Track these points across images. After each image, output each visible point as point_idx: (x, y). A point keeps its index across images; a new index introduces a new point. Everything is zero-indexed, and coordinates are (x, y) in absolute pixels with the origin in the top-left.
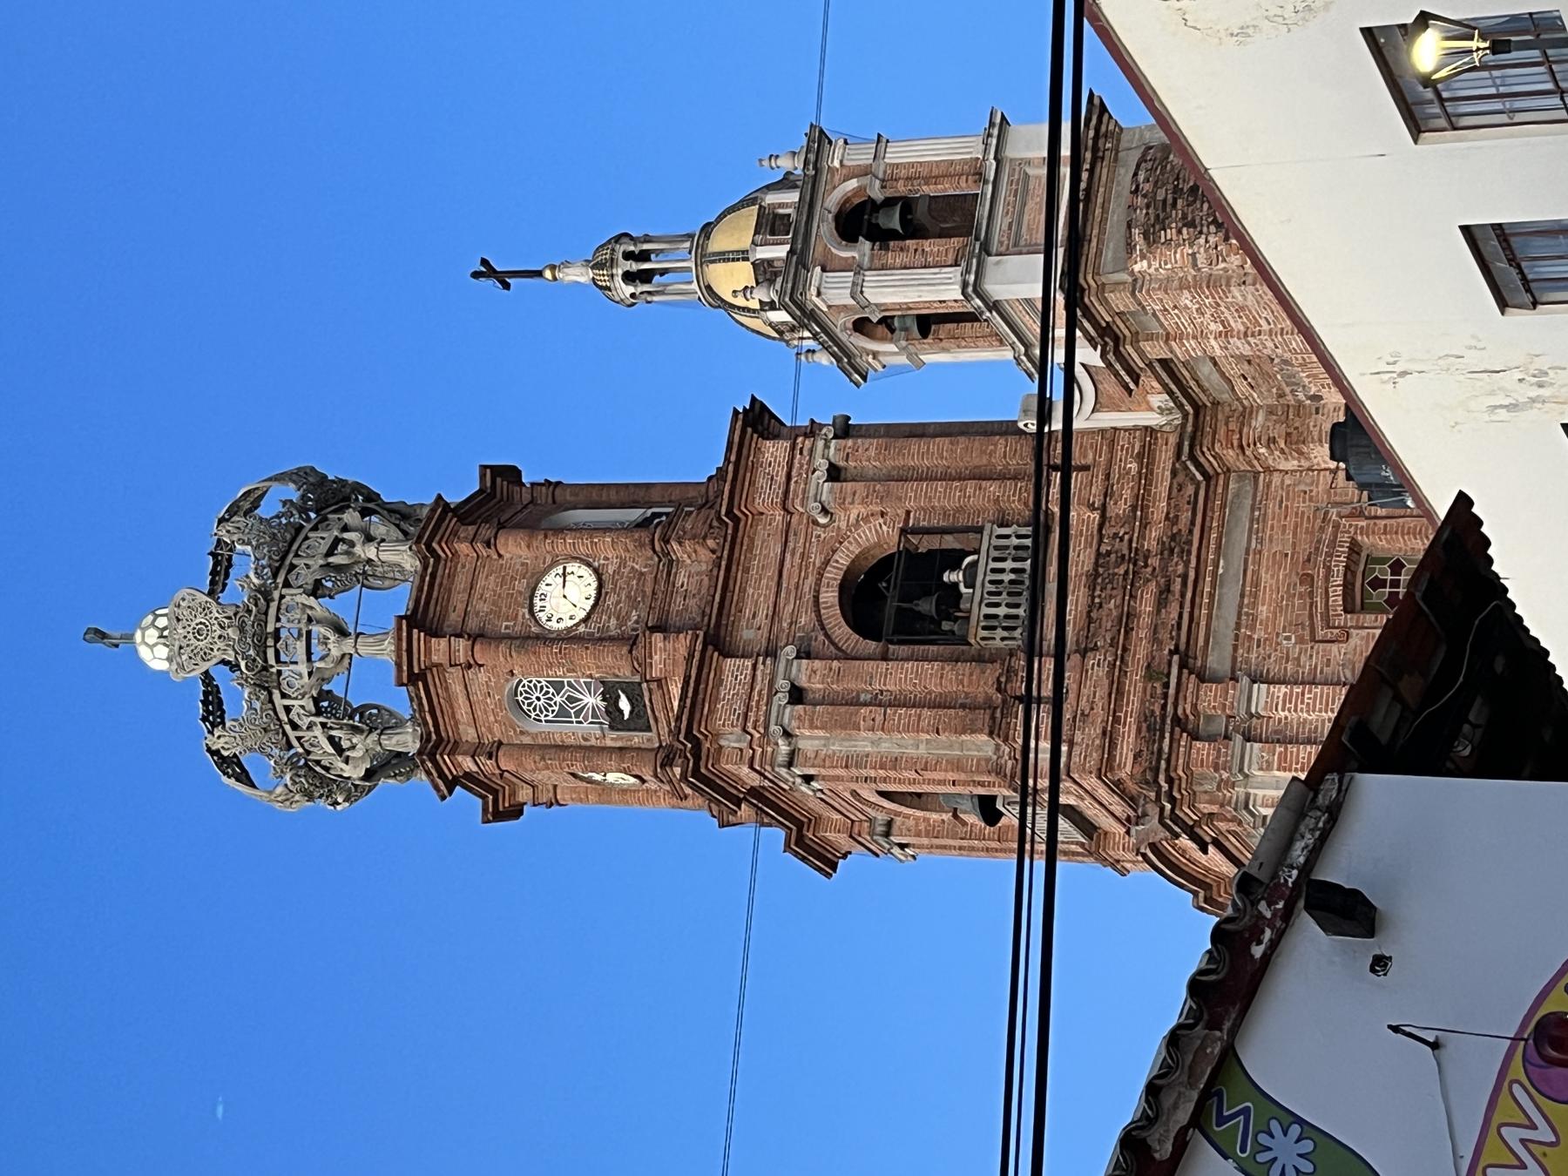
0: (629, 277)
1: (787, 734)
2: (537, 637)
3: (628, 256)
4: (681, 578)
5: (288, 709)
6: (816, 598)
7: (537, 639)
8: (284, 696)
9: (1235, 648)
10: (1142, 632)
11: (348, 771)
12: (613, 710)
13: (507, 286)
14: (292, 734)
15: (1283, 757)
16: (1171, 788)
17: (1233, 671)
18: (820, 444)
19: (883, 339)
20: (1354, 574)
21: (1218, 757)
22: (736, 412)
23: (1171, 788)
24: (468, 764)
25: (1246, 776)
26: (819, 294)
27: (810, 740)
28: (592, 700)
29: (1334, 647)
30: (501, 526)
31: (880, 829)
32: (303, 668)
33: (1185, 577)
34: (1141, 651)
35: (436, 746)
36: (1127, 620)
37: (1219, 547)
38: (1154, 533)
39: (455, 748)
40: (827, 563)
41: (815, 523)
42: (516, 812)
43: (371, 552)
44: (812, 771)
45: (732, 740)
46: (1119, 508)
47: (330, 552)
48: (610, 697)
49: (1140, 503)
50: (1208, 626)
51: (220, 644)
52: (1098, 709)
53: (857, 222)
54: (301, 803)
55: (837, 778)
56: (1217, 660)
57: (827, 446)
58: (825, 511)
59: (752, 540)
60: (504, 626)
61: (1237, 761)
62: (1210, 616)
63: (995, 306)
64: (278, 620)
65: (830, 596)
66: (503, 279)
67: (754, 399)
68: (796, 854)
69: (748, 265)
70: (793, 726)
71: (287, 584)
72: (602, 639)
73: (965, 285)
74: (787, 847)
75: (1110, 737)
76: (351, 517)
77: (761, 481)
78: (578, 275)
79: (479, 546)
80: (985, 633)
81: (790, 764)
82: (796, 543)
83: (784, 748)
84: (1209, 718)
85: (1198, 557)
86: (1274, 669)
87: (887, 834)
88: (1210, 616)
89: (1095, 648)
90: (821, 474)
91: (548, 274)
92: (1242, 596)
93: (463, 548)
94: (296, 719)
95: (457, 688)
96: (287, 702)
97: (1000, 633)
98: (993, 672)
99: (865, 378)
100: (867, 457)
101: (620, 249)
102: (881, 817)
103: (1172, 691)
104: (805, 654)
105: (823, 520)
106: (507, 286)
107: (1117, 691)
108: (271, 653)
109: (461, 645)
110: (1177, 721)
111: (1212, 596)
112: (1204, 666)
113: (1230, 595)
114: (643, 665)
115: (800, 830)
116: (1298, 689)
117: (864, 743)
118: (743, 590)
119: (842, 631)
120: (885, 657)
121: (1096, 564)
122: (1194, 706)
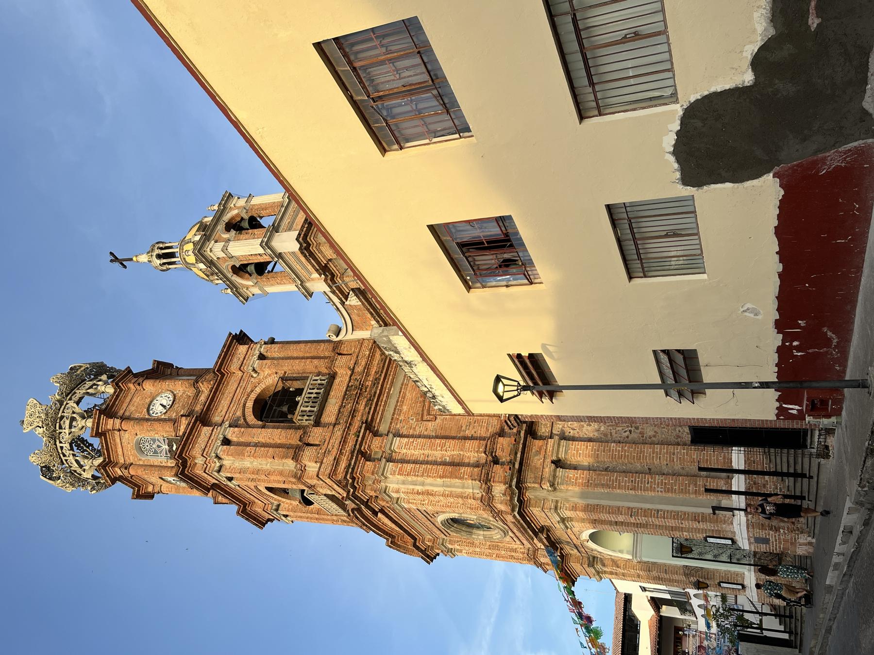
0: (159, 257)
1: (217, 457)
2: (147, 420)
3: (161, 249)
5: (62, 448)
9: (391, 423)
13: (125, 267)
14: (63, 458)
15: (401, 469)
16: (353, 482)
17: (389, 432)
18: (259, 346)
19: (247, 279)
22: (230, 334)
23: (353, 482)
25: (386, 478)
26: (211, 251)
27: (227, 462)
28: (166, 447)
29: (430, 423)
30: (147, 378)
31: (274, 507)
32: (67, 431)
33: (375, 393)
34: (356, 423)
35: (107, 464)
36: (353, 413)
37: (392, 382)
38: (371, 378)
39: (116, 464)
40: (252, 391)
42: (150, 496)
44: (229, 475)
45: (200, 461)
46: (359, 369)
47: (91, 387)
49: (367, 367)
50: (382, 414)
51: (38, 420)
52: (335, 450)
54: (70, 489)
55: (241, 479)
56: (383, 429)
58: (256, 372)
59: (228, 383)
60: (137, 415)
61: (381, 470)
62: (383, 410)
63: (280, 256)
65: (250, 404)
67: (241, 331)
69: (191, 244)
70: (221, 454)
71: (70, 399)
73: (262, 241)
75: (337, 461)
76: (104, 377)
77: (235, 360)
78: (143, 258)
81: (219, 471)
82: (243, 384)
83: (218, 464)
84: (376, 453)
85: (382, 386)
87: (277, 510)
89: (339, 424)
90: (256, 357)
91: (134, 259)
92: (397, 402)
93: (131, 385)
94: (64, 451)
95: (118, 440)
97: (306, 417)
98: (300, 432)
99: (246, 300)
100: (274, 351)
101: (157, 246)
102: (276, 503)
103: (360, 439)
105: (255, 375)
106: (125, 267)
107: (344, 441)
108: (58, 425)
109: (118, 421)
110: (360, 451)
111: (386, 402)
112: (378, 430)
113: (392, 402)
114: (176, 430)
115: (245, 507)
116: (411, 440)
118: (220, 401)
119: (251, 418)
120: (263, 427)
122: (369, 446)
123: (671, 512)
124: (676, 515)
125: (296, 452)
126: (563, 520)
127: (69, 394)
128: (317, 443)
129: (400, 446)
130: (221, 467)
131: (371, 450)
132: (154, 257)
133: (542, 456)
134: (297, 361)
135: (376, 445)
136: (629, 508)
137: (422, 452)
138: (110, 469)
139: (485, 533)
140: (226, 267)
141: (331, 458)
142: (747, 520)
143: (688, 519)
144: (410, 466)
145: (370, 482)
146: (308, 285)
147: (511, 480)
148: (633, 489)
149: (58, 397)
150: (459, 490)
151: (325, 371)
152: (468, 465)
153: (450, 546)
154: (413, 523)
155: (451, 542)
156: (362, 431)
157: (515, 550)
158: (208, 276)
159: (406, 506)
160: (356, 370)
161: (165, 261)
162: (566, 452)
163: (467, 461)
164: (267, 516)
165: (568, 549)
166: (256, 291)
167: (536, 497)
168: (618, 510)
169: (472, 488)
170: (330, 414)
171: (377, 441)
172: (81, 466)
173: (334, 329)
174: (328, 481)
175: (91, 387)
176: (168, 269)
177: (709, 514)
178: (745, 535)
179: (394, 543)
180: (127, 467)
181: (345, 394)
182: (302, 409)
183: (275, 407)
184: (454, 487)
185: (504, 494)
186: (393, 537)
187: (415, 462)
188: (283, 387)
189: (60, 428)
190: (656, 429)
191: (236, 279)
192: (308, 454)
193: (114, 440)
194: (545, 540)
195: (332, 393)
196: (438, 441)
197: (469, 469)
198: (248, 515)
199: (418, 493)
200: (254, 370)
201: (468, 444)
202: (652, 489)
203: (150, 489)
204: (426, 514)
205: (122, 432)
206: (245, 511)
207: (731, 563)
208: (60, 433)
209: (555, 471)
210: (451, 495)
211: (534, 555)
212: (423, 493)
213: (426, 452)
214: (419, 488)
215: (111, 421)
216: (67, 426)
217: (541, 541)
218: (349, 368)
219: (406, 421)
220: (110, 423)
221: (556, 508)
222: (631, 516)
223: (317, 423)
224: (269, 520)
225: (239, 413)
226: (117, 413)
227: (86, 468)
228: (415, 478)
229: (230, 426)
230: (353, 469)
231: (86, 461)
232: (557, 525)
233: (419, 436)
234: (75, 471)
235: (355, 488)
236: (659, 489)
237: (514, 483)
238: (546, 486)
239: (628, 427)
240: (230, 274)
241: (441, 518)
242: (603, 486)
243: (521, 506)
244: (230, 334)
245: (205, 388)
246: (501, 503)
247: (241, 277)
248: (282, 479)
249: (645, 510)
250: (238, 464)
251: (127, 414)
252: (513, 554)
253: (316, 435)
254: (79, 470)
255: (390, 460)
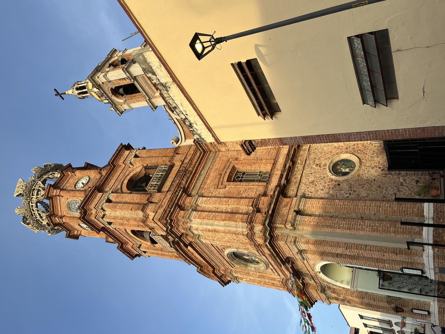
0: (77, 89)
5: (32, 206)
6: (123, 182)
8: (32, 203)
9: (199, 190)
13: (63, 99)
14: (33, 212)
15: (200, 215)
20: (233, 175)
21: (184, 215)
22: (121, 144)
25: (191, 221)
26: (98, 78)
29: (222, 190)
32: (35, 197)
39: (57, 216)
40: (128, 175)
41: (130, 167)
45: (94, 211)
46: (186, 161)
47: (51, 174)
49: (191, 160)
51: (21, 190)
54: (36, 231)
56: (194, 193)
57: (136, 151)
58: (132, 165)
59: (117, 171)
60: (69, 188)
61: (188, 215)
62: (196, 183)
64: (35, 187)
65: (126, 182)
67: (129, 144)
68: (121, 251)
70: (104, 207)
71: (40, 180)
74: (118, 248)
80: (149, 188)
82: (124, 171)
83: (103, 214)
84: (188, 206)
87: (139, 248)
88: (196, 183)
90: (133, 156)
91: (66, 92)
92: (204, 178)
93: (69, 173)
96: (32, 204)
98: (148, 196)
100: (143, 154)
102: (139, 243)
103: (178, 197)
105: (131, 167)
109: (58, 191)
110: (177, 204)
112: (191, 194)
113: (202, 178)
116: (209, 199)
119: (125, 189)
121: (177, 173)
123: (376, 247)
124: (380, 249)
126: (301, 252)
127: (40, 177)
128: (157, 202)
129: (202, 203)
130: (104, 215)
131: (185, 205)
132: (75, 89)
133: (288, 208)
135: (188, 201)
136: (345, 243)
137: (214, 206)
138: (53, 218)
139: (256, 266)
140: (107, 89)
141: (162, 210)
142: (434, 253)
143: (388, 252)
145: (182, 223)
146: (153, 100)
147: (265, 220)
148: (349, 229)
149: (33, 179)
150: (234, 229)
152: (242, 213)
153: (236, 275)
154: (212, 257)
155: (236, 272)
156: (181, 192)
157: (274, 279)
158: (99, 97)
159: (204, 241)
160: (185, 162)
161: (80, 91)
162: (304, 206)
163: (241, 211)
164: (136, 253)
165: (308, 280)
166: (126, 107)
167: (281, 233)
168: (338, 245)
169: (242, 228)
171: (189, 199)
172: (41, 217)
173: (175, 138)
174: (159, 223)
175: (51, 174)
176: (84, 97)
177: (405, 249)
178: (432, 266)
179: (201, 270)
180: (61, 217)
181: (177, 174)
182: (152, 183)
184: (231, 227)
185: (261, 232)
186: (202, 267)
188: (146, 174)
189: (33, 195)
190: (368, 192)
191: (114, 98)
193: (57, 202)
194: (290, 269)
196: (225, 199)
197: (241, 216)
198: (124, 250)
199: (209, 231)
200: (131, 163)
201: (242, 201)
202: (362, 229)
203: (76, 233)
204: (217, 248)
205: (61, 197)
206: (122, 247)
207: (421, 294)
208: (32, 198)
209: (295, 217)
210: (229, 232)
211: (286, 282)
212: (212, 231)
213: (217, 206)
214: (210, 228)
215: (55, 191)
217: (287, 269)
218: (181, 161)
219: (208, 188)
220: (55, 192)
221: (295, 242)
222: (347, 248)
224: (137, 255)
225: (119, 187)
226: (60, 187)
227: (44, 218)
228: (208, 221)
229: (112, 192)
230: (172, 214)
231: (43, 214)
232: (297, 257)
234: (39, 220)
235: (172, 226)
236: (368, 229)
237: (267, 222)
238: (289, 226)
239: (348, 191)
240: (110, 95)
241: (227, 252)
242: (327, 226)
243: (272, 239)
244: (121, 144)
246: (259, 238)
247: (117, 97)
248: (136, 223)
249: (357, 245)
250: (113, 214)
251: (65, 188)
252: (273, 282)
253: (157, 197)
254: (41, 220)
255: (195, 210)
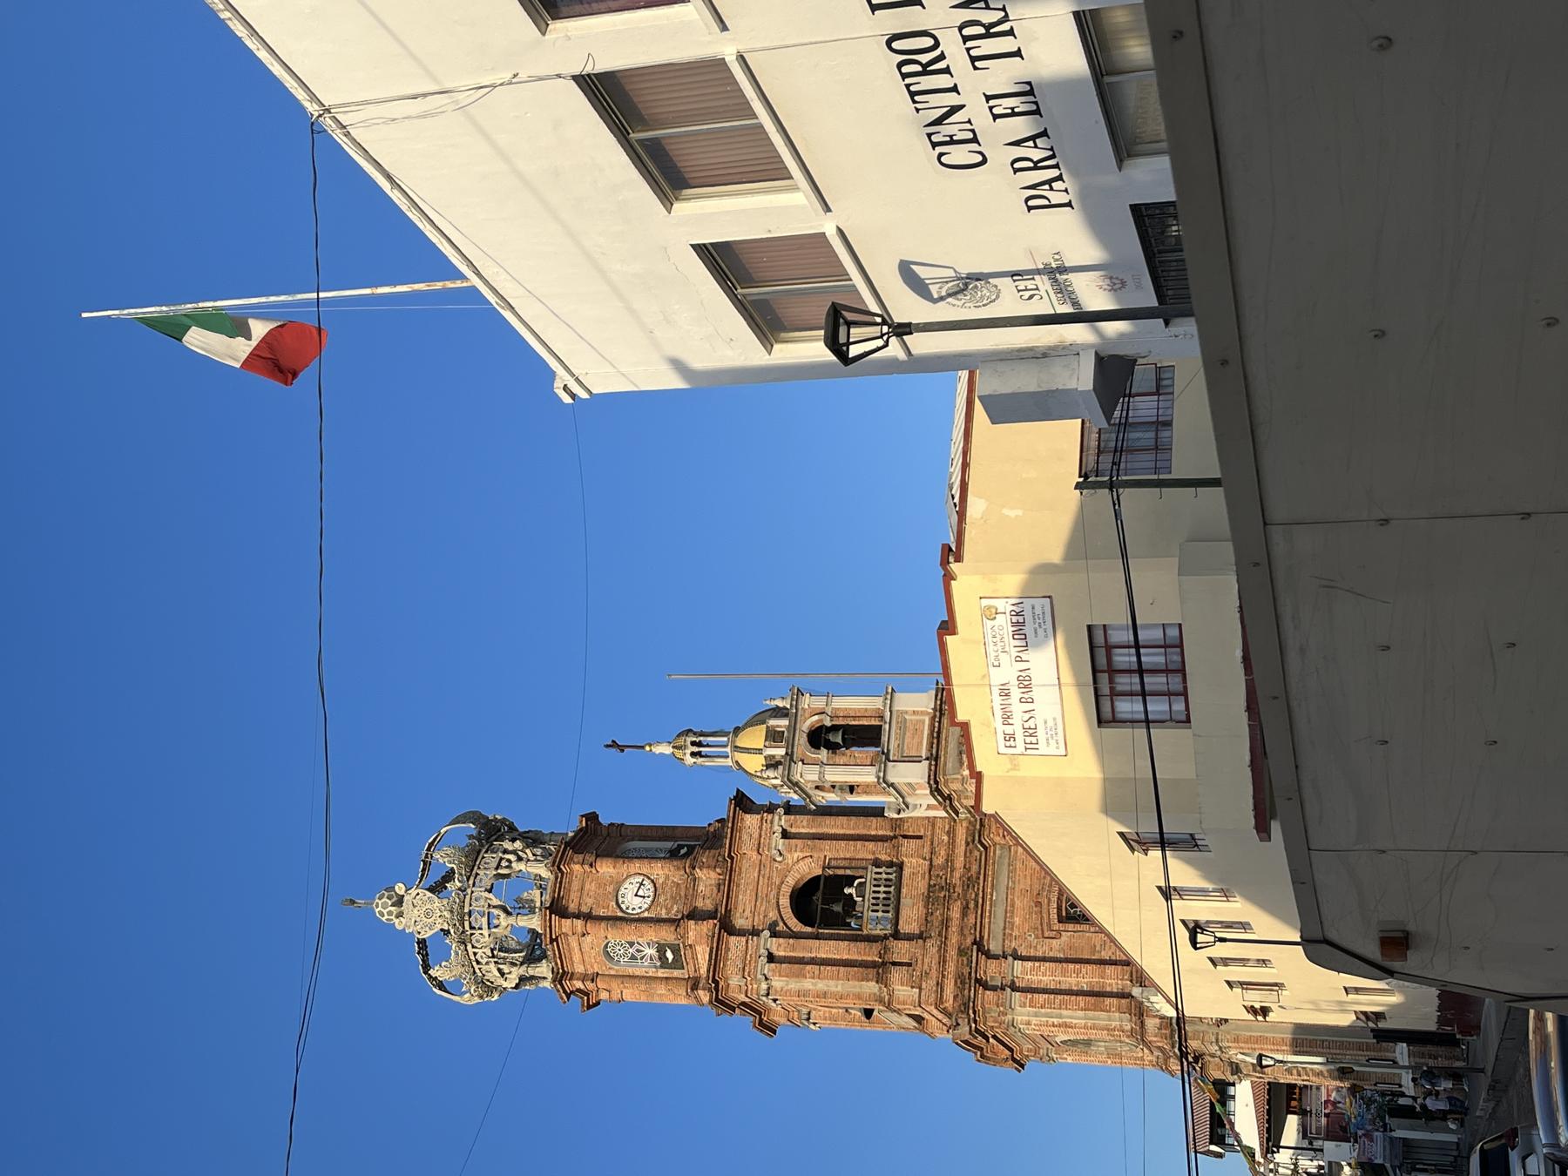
0: (693, 754)
2: (621, 919)
3: (693, 744)
4: (701, 888)
7: (622, 919)
10: (954, 929)
11: (505, 984)
12: (662, 957)
15: (1031, 1001)
24: (579, 985)
27: (777, 983)
28: (651, 951)
32: (485, 932)
34: (954, 939)
36: (946, 923)
38: (957, 874)
43: (521, 866)
45: (735, 981)
46: (939, 861)
48: (661, 950)
49: (950, 859)
53: (818, 738)
56: (994, 947)
63: (892, 785)
65: (785, 902)
66: (621, 748)
70: (769, 975)
72: (658, 921)
75: (940, 985)
77: (745, 837)
79: (587, 867)
83: (764, 986)
86: (1023, 952)
90: (778, 835)
93: (577, 867)
95: (574, 944)
98: (876, 947)
100: (802, 825)
102: (805, 1011)
104: (774, 934)
107: (943, 961)
109: (579, 923)
113: (1000, 911)
117: (807, 984)
120: (817, 937)
125: (880, 969)
129: (1022, 972)
134: (843, 843)
138: (567, 984)
144: (1042, 998)
151: (884, 857)
170: (911, 919)
171: (992, 964)
183: (821, 904)
187: (1045, 991)
189: (472, 928)
192: (896, 975)
195: (904, 891)
196: (1071, 966)
197: (1115, 1001)
201: (1109, 970)
210: (1094, 1027)
215: (567, 923)
216: (485, 926)
219: (1023, 937)
223: (896, 935)
233: (1044, 959)
245: (707, 878)
251: (585, 909)
253: (901, 950)
255: (1014, 988)
